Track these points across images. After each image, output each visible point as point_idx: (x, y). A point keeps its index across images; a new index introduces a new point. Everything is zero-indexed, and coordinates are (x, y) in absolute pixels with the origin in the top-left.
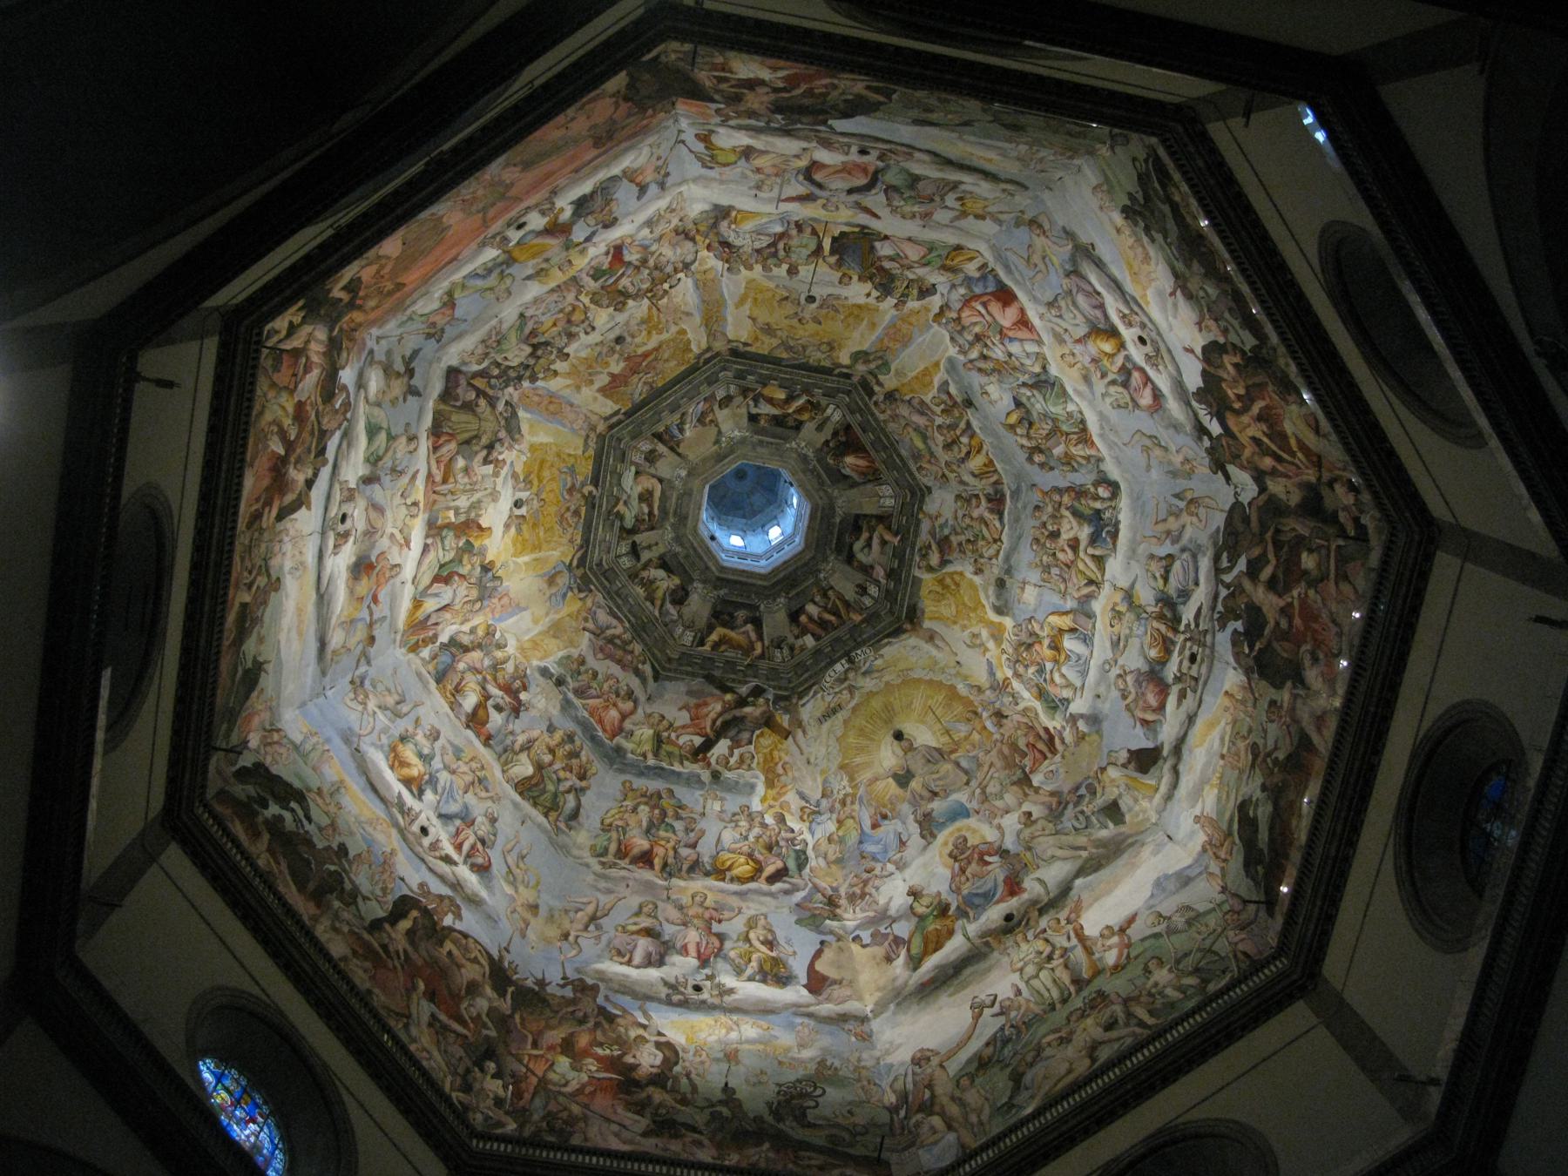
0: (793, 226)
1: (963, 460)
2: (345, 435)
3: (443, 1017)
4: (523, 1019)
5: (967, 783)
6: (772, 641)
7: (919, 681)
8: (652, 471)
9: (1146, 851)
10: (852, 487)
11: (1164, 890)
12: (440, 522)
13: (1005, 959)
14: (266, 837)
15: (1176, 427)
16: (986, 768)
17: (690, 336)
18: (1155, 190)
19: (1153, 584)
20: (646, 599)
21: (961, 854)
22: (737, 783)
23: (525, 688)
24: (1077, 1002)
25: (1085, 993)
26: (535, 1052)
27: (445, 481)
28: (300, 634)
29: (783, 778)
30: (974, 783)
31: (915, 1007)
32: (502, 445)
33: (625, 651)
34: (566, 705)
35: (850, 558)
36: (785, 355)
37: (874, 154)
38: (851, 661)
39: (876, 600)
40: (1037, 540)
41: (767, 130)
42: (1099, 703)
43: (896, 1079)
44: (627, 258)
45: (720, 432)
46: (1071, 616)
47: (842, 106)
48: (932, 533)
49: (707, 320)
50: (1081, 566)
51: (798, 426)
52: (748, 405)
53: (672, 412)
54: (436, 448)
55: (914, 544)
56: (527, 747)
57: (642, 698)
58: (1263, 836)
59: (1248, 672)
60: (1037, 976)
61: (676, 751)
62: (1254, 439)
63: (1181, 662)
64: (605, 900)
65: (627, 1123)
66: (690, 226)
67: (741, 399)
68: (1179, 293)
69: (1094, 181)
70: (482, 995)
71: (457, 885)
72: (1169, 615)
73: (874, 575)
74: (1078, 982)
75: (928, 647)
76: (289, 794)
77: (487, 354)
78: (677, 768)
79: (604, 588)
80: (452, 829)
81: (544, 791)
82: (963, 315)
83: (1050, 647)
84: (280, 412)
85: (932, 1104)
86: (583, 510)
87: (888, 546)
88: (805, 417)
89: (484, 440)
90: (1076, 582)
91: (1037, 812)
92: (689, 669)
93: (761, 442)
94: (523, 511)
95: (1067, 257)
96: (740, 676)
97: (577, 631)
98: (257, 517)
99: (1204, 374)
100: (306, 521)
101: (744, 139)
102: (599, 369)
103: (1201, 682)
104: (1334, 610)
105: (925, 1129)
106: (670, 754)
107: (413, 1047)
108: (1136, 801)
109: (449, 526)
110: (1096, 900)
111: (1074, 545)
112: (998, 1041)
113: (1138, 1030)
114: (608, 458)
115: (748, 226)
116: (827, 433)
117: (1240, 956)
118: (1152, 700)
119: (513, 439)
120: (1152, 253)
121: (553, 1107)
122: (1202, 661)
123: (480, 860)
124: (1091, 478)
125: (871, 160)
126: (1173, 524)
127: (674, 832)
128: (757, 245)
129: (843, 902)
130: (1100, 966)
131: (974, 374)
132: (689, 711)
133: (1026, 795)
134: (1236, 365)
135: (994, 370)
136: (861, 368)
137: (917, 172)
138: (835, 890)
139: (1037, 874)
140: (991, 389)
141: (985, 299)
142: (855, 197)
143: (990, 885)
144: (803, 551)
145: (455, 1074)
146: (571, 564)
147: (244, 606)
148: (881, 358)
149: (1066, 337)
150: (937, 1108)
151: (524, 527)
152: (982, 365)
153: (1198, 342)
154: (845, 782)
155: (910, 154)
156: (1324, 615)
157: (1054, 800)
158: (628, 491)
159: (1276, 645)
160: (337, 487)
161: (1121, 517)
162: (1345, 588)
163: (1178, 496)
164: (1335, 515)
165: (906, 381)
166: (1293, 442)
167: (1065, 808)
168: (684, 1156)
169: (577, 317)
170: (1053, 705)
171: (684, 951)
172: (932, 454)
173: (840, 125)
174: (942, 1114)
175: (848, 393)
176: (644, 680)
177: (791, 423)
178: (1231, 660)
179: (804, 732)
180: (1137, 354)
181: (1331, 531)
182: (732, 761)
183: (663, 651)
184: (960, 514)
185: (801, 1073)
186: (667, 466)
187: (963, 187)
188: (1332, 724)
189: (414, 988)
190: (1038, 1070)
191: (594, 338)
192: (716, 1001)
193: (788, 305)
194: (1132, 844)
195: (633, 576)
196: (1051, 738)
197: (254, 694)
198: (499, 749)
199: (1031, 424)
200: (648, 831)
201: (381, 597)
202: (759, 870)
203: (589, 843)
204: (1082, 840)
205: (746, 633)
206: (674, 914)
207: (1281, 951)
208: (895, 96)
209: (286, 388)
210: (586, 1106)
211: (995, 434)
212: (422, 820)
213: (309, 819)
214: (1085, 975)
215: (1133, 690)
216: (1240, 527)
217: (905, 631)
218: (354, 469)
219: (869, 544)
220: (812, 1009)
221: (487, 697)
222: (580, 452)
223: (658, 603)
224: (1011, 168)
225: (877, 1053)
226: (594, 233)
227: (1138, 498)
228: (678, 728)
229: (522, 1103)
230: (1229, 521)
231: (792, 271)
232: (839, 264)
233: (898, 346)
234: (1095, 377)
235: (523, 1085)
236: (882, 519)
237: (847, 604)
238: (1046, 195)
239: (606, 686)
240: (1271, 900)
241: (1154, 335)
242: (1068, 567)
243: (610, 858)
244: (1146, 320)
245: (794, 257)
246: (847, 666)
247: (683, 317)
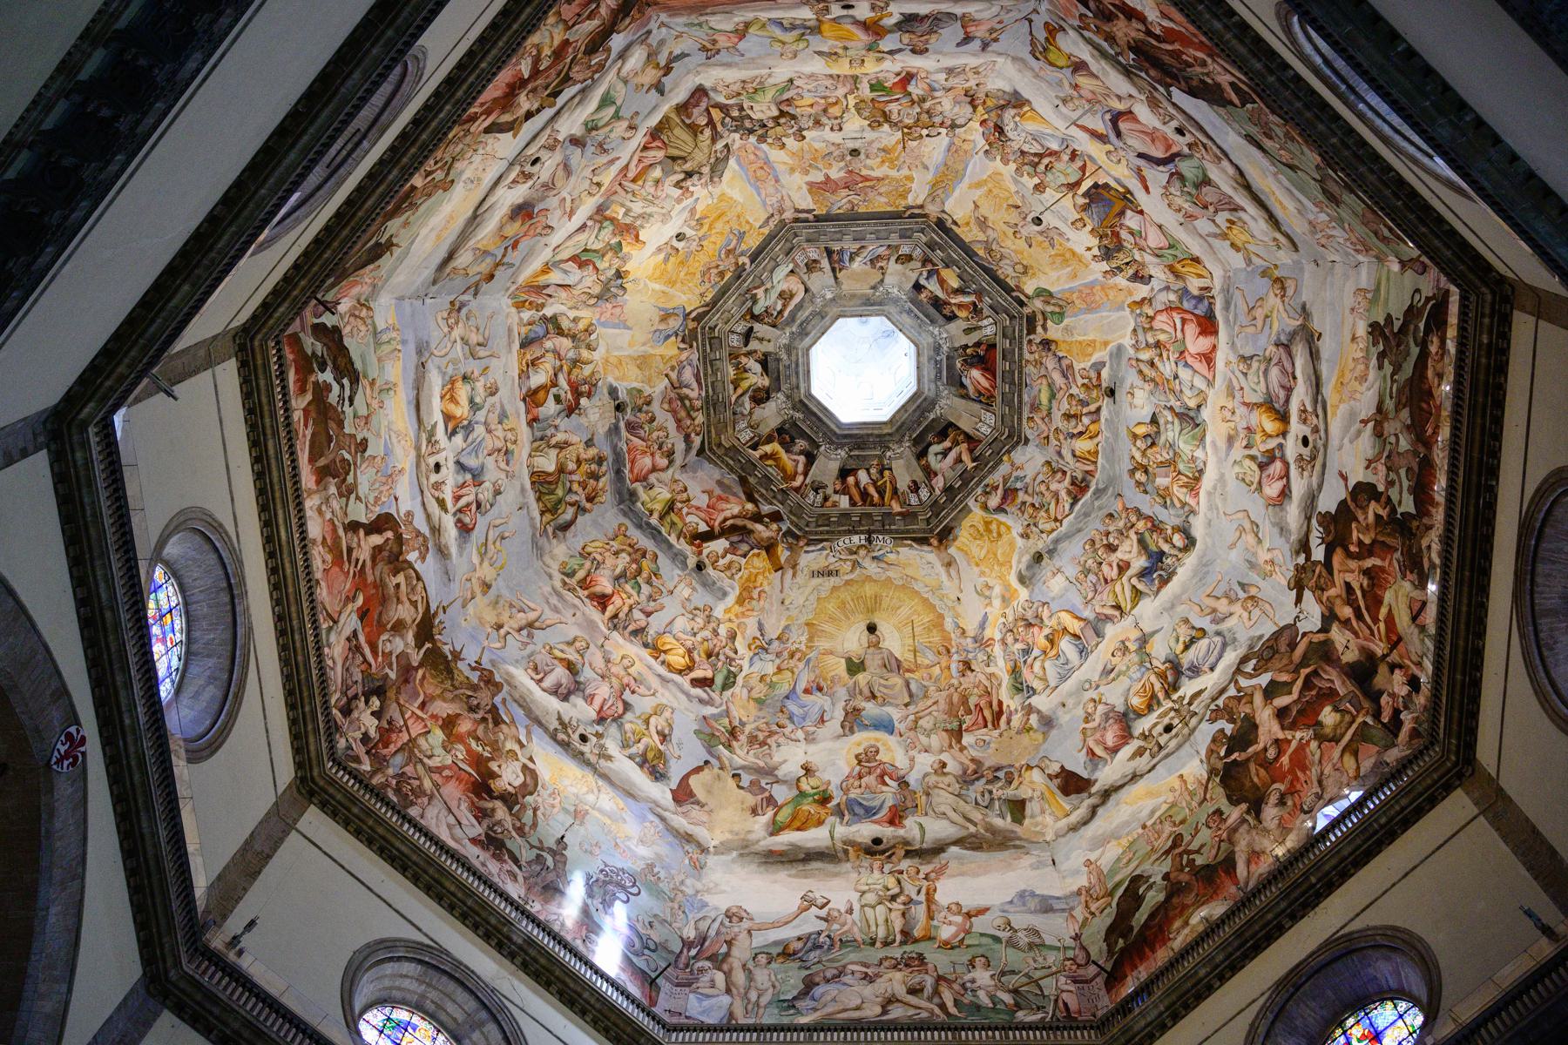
0: (1069, 151)
1: (1073, 436)
2: (583, 91)
3: (362, 638)
4: (424, 677)
5: (906, 705)
8: (805, 277)
9: (1027, 861)
10: (962, 397)
11: (1024, 904)
12: (608, 213)
13: (854, 875)
14: (309, 397)
15: (1283, 530)
16: (929, 703)
17: (914, 186)
18: (1417, 327)
19: (1173, 644)
21: (867, 760)
23: (589, 395)
24: (896, 952)
25: (908, 948)
26: (419, 713)
27: (634, 181)
28: (438, 237)
30: (912, 708)
31: (753, 867)
34: (615, 430)
36: (981, 253)
37: (1188, 138)
38: (869, 540)
39: (921, 503)
40: (1093, 542)
41: (1113, 60)
42: (1060, 711)
43: (703, 918)
44: (910, 88)
46: (1082, 624)
47: (1195, 83)
48: (1005, 480)
50: (1118, 588)
51: (951, 318)
54: (645, 148)
55: (985, 477)
56: (562, 446)
58: (1141, 916)
59: (1212, 772)
60: (873, 907)
61: (680, 525)
62: (1348, 586)
63: (1155, 725)
64: (550, 617)
65: (464, 822)
66: (981, 95)
68: (1371, 425)
69: (1364, 284)
70: (402, 637)
71: (436, 530)
72: (1170, 679)
74: (906, 934)
75: (942, 570)
76: (348, 371)
77: (739, 94)
78: (672, 539)
80: (460, 480)
81: (552, 492)
82: (1159, 317)
83: (1047, 637)
84: (547, 40)
85: (723, 961)
86: (728, 276)
88: (962, 314)
89: (688, 166)
90: (1105, 600)
91: (952, 767)
93: (910, 312)
94: (680, 245)
95: (1287, 330)
96: (769, 495)
97: (660, 373)
98: (473, 118)
99: (1343, 504)
100: (506, 145)
101: (1085, 53)
103: (1163, 753)
104: (1326, 772)
105: (705, 979)
106: (673, 524)
107: (326, 650)
108: (1043, 812)
109: (612, 220)
110: (962, 874)
111: (1123, 567)
112: (811, 942)
113: (937, 1011)
115: (1031, 126)
117: (1061, 1004)
118: (1110, 739)
120: (1372, 374)
121: (409, 770)
122: (1176, 735)
123: (467, 520)
124: (1177, 522)
125: (1181, 143)
126: (1222, 606)
128: (1026, 148)
129: (743, 738)
130: (933, 933)
131: (1133, 372)
133: (951, 746)
134: (1378, 517)
135: (1153, 380)
136: (1038, 304)
137: (1212, 176)
138: (743, 724)
139: (922, 820)
140: (1138, 393)
141: (1188, 316)
142: (1141, 162)
143: (876, 803)
144: (884, 423)
145: (344, 693)
147: (413, 188)
149: (1238, 395)
150: (725, 967)
151: (672, 259)
152: (1147, 370)
153: (1358, 475)
154: (804, 639)
155: (1220, 159)
156: (1314, 772)
157: (972, 767)
159: (1252, 767)
160: (548, 131)
161: (1180, 570)
162: (1349, 762)
163: (1243, 586)
164: (1381, 693)
165: (1069, 339)
166: (1383, 611)
167: (977, 779)
168: (496, 879)
169: (835, 111)
170: (1019, 687)
171: (590, 699)
172: (1049, 414)
173: (1178, 96)
174: (728, 975)
175: (1012, 318)
176: (688, 449)
178: (1203, 753)
179: (794, 575)
180: (1292, 449)
181: (1366, 704)
182: (722, 562)
183: (718, 435)
184: (1040, 478)
185: (627, 864)
186: (821, 281)
187: (1241, 214)
188: (1264, 867)
189: (354, 599)
190: (831, 990)
191: (836, 137)
192: (593, 759)
193: (1015, 212)
194: (1016, 847)
195: (734, 356)
196: (1000, 713)
197: (371, 267)
198: (538, 434)
199: (1153, 444)
200: (617, 578)
201: (520, 246)
202: (690, 669)
203: (562, 558)
204: (976, 816)
205: (797, 462)
206: (599, 663)
207: (1101, 1025)
208: (1249, 106)
209: (565, 22)
210: (437, 786)
211: (1116, 435)
212: (440, 458)
213: (351, 404)
214: (917, 933)
215: (1098, 717)
216: (1283, 648)
218: (570, 125)
219: (945, 453)
220: (666, 814)
221: (555, 384)
223: (740, 391)
224: (1297, 227)
225: (699, 886)
226: (900, 50)
227: (1205, 565)
229: (385, 751)
230: (1276, 636)
231: (1039, 188)
232: (1085, 208)
234: (1240, 444)
235: (394, 736)
236: (969, 438)
237: (895, 491)
238: (1309, 268)
239: (655, 435)
240: (1113, 979)
241: (1320, 443)
242: (1106, 581)
243: (573, 582)
244: (1322, 427)
245: (1050, 177)
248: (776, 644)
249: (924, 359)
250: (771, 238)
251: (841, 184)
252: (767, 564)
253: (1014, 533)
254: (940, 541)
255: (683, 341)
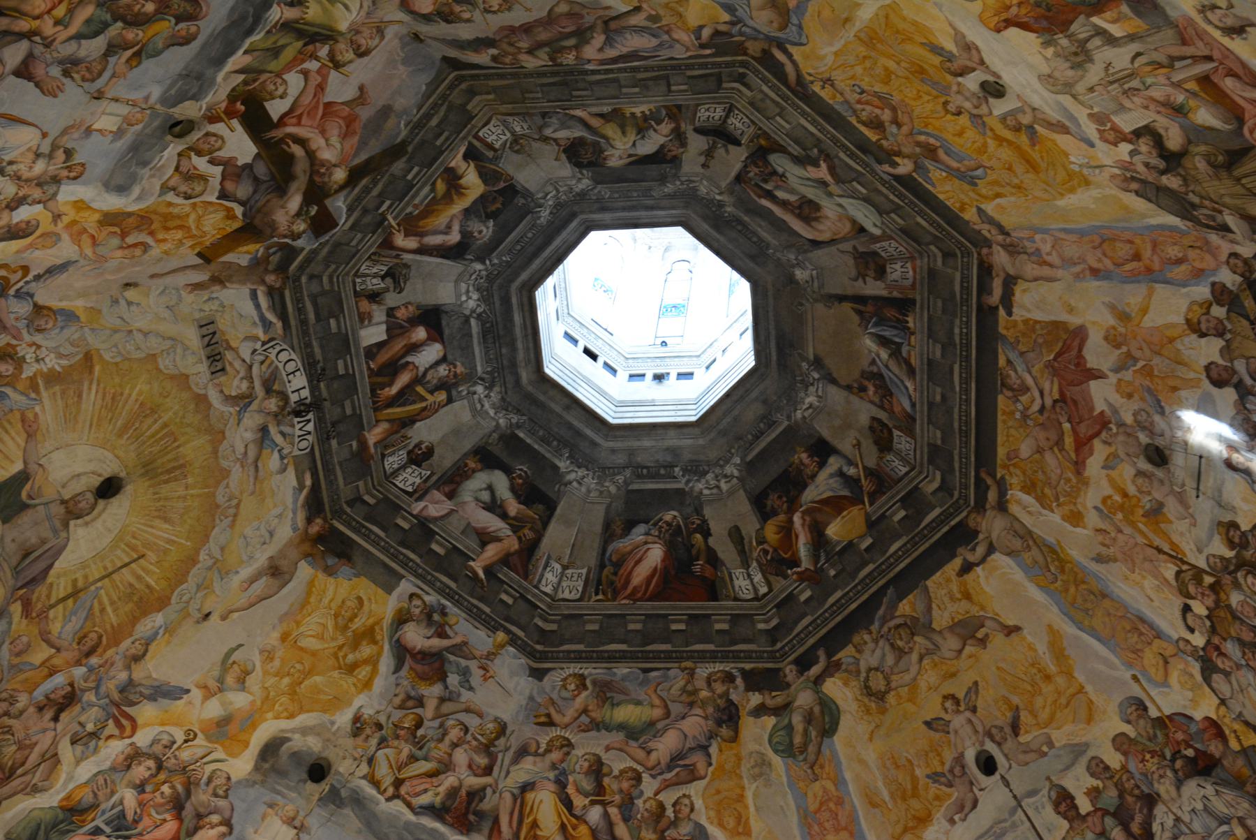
1: (561, 784)
6: (407, 266)
7: (207, 537)
8: (847, 246)
10: (607, 525)
12: (1125, 8)
17: (1056, 517)
20: (615, 111)
22: (145, 164)
29: (116, 241)
32: (1147, 165)
33: (540, 45)
35: (486, 457)
36: (905, 607)
38: (300, 411)
45: (834, 381)
48: (460, 649)
49: (1059, 559)
51: (764, 514)
52: (850, 463)
53: (930, 363)
55: (457, 603)
57: (424, 29)
61: (274, 65)
67: (871, 462)
73: (436, 495)
75: (261, 560)
78: (238, 59)
79: (690, 67)
87: (473, 543)
88: (771, 532)
92: (434, 122)
94: (972, 82)
96: (369, 201)
102: (1128, 375)
106: (276, 52)
114: (932, 223)
116: (726, 552)
119: (1143, 182)
127: (79, 37)
132: (342, 103)
136: (804, 699)
146: (790, 56)
148: (804, 749)
151: (936, 60)
154: (52, 362)
158: (843, 201)
165: (745, 769)
172: (596, 725)
175: (773, 636)
177: (773, 500)
182: (201, 163)
183: (494, 90)
184: (473, 721)
193: (1002, 718)
195: (675, 113)
205: (446, 233)
217: (309, 521)
219: (494, 507)
222: (989, 208)
228: (325, 78)
231: (1064, 801)
233: (812, 808)
236: (529, 550)
237: (409, 421)
246: (294, 398)
247: (1104, 550)
248: (23, 308)
249: (672, 440)
250: (952, 219)
251: (1072, 392)
252: (208, 241)
253: (359, 701)
254: (320, 539)
255: (717, 33)
